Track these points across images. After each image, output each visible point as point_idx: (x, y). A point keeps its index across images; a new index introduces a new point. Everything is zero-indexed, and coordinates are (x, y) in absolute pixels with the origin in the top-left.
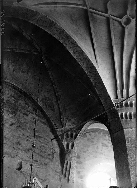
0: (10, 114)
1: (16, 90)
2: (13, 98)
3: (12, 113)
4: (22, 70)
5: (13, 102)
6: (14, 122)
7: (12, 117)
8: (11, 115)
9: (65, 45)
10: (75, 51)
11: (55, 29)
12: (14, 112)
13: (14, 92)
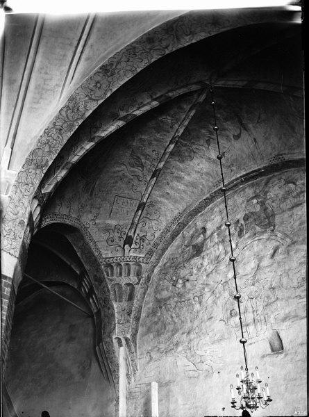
0: (261, 237)
1: (253, 177)
2: (255, 201)
3: (263, 233)
4: (234, 136)
5: (258, 208)
6: (278, 243)
7: (268, 239)
8: (265, 236)
9: (166, 50)
10: (189, 32)
11: (123, 64)
12: (270, 224)
13: (252, 185)
